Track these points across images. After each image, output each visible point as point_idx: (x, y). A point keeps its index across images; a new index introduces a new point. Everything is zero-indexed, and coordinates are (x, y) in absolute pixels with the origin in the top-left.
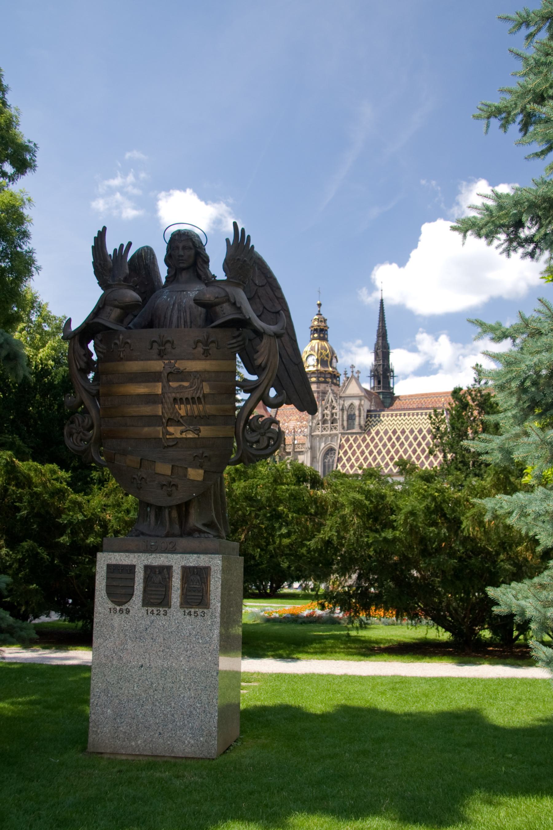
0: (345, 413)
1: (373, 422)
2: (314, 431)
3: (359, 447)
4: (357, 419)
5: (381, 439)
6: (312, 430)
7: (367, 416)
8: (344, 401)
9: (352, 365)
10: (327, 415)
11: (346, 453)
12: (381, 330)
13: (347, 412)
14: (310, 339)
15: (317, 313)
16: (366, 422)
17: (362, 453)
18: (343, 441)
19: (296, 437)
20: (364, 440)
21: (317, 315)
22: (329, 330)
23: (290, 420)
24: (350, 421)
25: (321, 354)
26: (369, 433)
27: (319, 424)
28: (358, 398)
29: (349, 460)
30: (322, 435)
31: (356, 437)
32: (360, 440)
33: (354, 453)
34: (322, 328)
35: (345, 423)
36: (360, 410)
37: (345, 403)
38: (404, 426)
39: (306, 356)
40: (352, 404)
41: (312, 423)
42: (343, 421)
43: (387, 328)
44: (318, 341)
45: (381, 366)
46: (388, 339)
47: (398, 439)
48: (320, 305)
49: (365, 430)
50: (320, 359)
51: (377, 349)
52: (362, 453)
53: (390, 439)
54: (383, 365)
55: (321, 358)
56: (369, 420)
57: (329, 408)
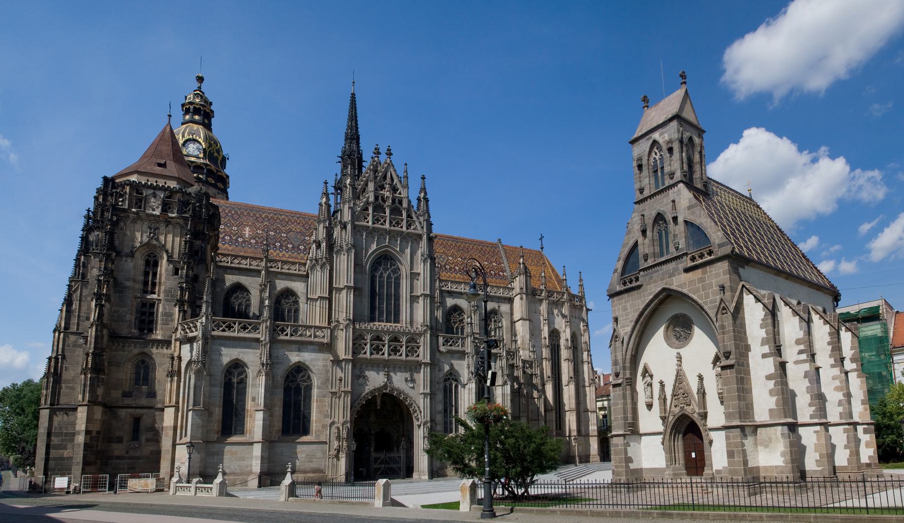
34: (207, 111)
48: (200, 79)
55: (210, 151)
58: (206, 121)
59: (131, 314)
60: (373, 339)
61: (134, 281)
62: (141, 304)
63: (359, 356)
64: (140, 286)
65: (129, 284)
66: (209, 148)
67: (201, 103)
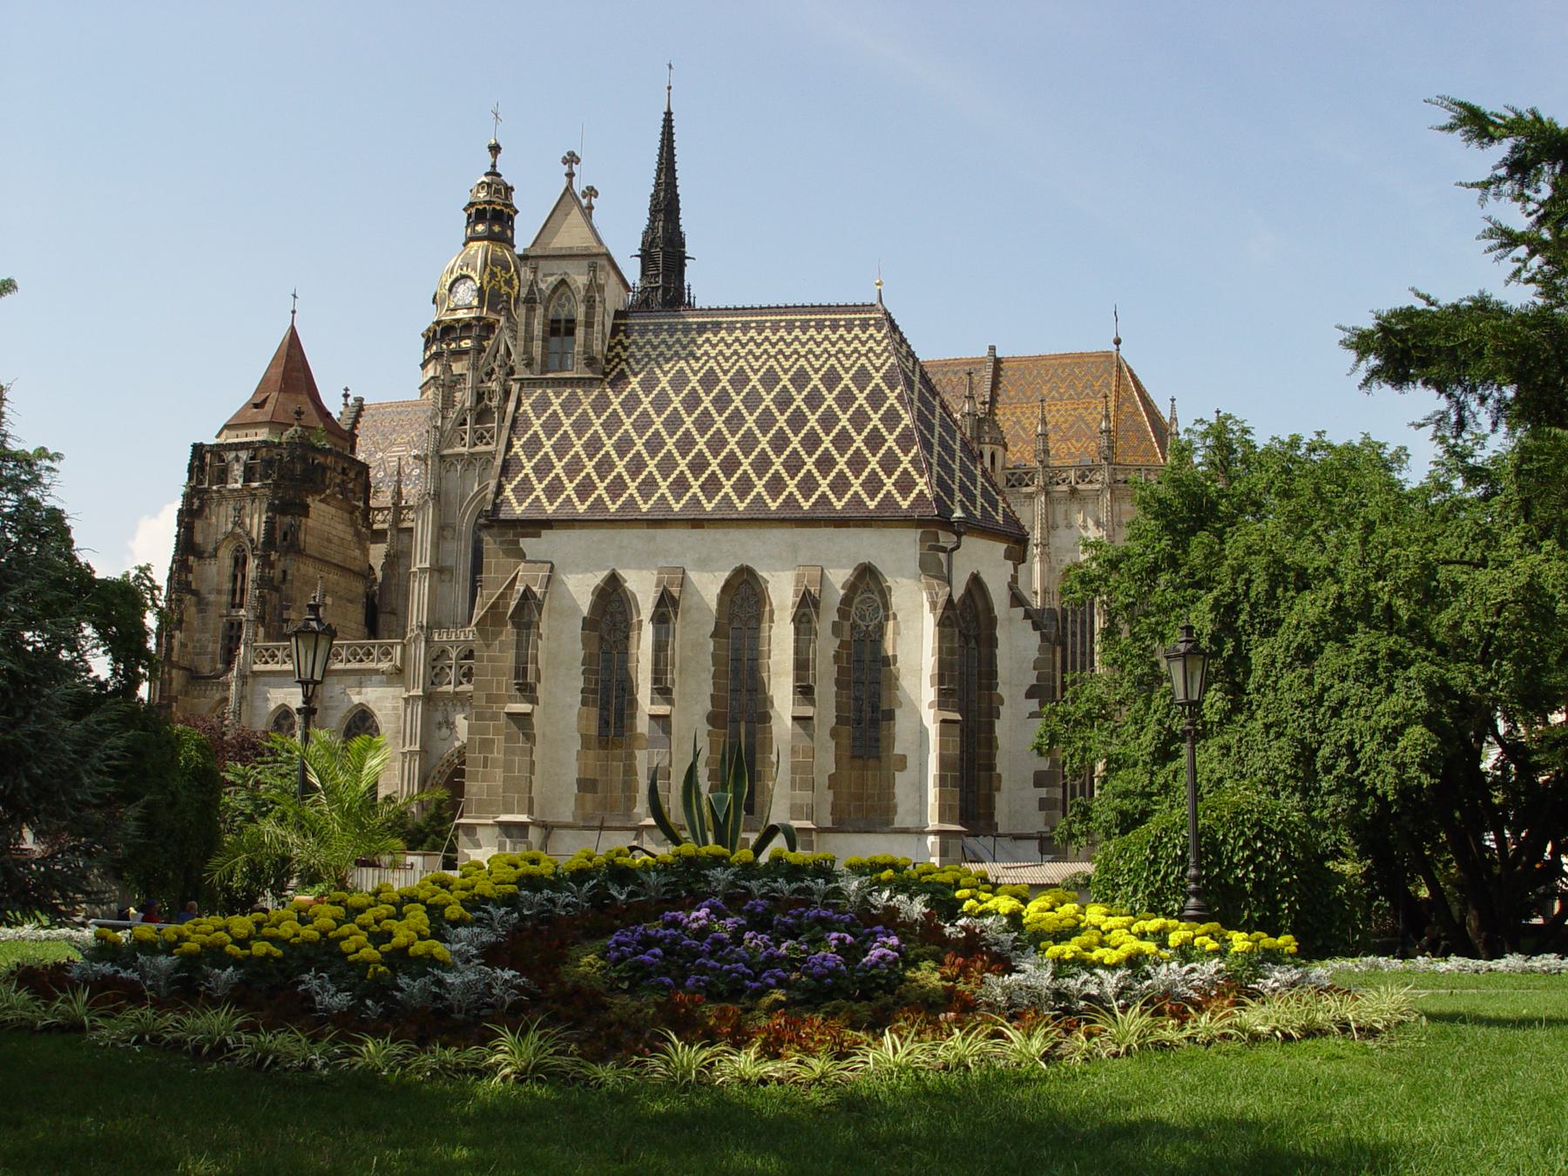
0: (540, 311)
1: (633, 349)
2: (450, 446)
3: (581, 426)
4: (580, 332)
6: (442, 439)
7: (615, 330)
8: (535, 271)
9: (572, 154)
10: (491, 393)
11: (534, 445)
12: (662, 194)
13: (546, 309)
14: (464, 240)
15: (489, 169)
16: (610, 349)
17: (593, 446)
19: (404, 492)
20: (601, 405)
21: (487, 174)
22: (516, 218)
23: (392, 444)
24: (555, 340)
27: (464, 423)
28: (585, 263)
29: (543, 468)
30: (472, 454)
31: (573, 394)
32: (586, 404)
33: (562, 448)
34: (498, 208)
35: (537, 349)
36: (590, 302)
37: (540, 275)
38: (742, 362)
39: (450, 281)
40: (563, 282)
41: (443, 418)
42: (529, 338)
43: (679, 191)
44: (486, 243)
45: (660, 291)
46: (681, 222)
47: (722, 401)
48: (495, 149)
49: (606, 374)
50: (487, 288)
51: (651, 247)
52: (593, 446)
53: (692, 402)
54: (666, 291)
55: (493, 287)
56: (620, 342)
57: (499, 373)
58: (497, 229)
59: (215, 642)
60: (462, 655)
61: (219, 592)
63: (439, 690)
64: (225, 598)
65: (212, 598)
66: (489, 282)
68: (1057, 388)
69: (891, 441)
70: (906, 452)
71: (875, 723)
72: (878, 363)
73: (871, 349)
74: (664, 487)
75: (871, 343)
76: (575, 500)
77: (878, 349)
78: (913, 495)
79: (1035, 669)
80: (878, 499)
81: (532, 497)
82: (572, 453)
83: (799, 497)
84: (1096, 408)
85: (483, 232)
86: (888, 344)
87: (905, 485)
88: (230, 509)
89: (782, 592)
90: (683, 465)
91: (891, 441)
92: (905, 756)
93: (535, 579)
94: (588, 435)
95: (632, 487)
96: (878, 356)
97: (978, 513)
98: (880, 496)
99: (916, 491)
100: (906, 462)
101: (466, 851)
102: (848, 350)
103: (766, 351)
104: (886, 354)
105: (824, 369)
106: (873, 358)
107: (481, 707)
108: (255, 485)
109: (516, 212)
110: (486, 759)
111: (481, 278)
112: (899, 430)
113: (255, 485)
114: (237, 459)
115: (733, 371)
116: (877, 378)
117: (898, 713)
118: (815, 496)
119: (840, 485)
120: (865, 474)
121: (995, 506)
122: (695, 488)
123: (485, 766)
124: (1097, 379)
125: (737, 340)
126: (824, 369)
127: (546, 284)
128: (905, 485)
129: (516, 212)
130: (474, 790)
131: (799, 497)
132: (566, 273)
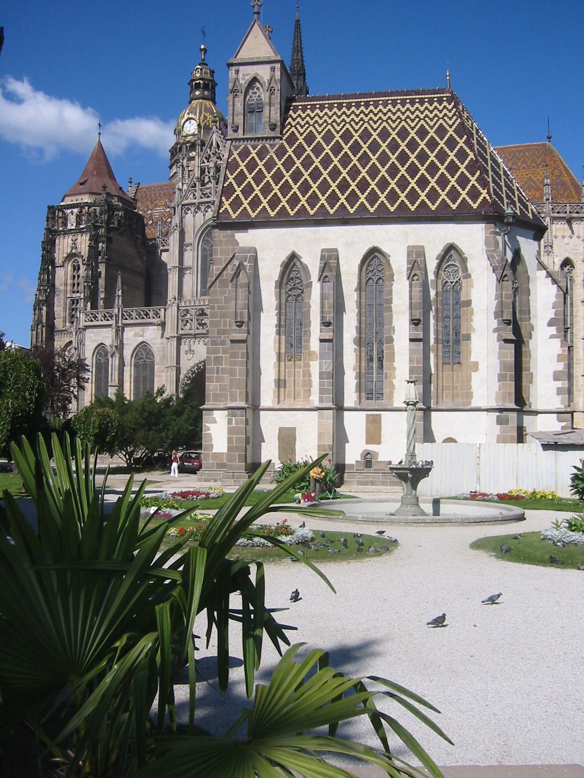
5: (318, 150)
8: (237, 72)
17: (278, 177)
18: (235, 154)
20: (281, 152)
23: (156, 206)
25: (205, 117)
26: (292, 139)
28: (268, 67)
31: (264, 147)
33: (259, 178)
37: (240, 75)
38: (366, 125)
47: (356, 148)
62: (71, 303)
66: (203, 121)
67: (201, 77)
68: (516, 164)
69: (462, 168)
70: (473, 175)
71: (457, 342)
72: (450, 123)
73: (445, 115)
74: (323, 200)
75: (445, 111)
76: (268, 209)
77: (450, 115)
78: (479, 201)
79: (553, 308)
80: (457, 203)
81: (242, 208)
82: (265, 181)
83: (408, 203)
84: (538, 173)
85: (199, 95)
86: (456, 111)
87: (474, 194)
88: (70, 240)
89: (399, 263)
90: (334, 186)
91: (462, 168)
92: (477, 363)
93: (245, 258)
94: (274, 171)
95: (303, 201)
96: (450, 119)
97: (518, 212)
98: (459, 201)
99: (481, 198)
100: (473, 180)
101: (207, 425)
102: (431, 116)
103: (380, 118)
104: (455, 117)
105: (417, 127)
106: (447, 120)
107: (214, 337)
108: (82, 226)
109: (217, 84)
110: (218, 368)
111: (199, 119)
112: (467, 162)
113: (82, 226)
114: (72, 213)
115: (361, 130)
116: (451, 131)
117: (473, 336)
118: (418, 203)
119: (433, 195)
120: (448, 188)
121: (526, 207)
122: (343, 199)
123: (218, 373)
124: (538, 158)
125: (362, 112)
126: (417, 127)
127: (243, 82)
128: (474, 194)
129: (217, 84)
130: (211, 388)
131: (408, 203)
132: (257, 73)
